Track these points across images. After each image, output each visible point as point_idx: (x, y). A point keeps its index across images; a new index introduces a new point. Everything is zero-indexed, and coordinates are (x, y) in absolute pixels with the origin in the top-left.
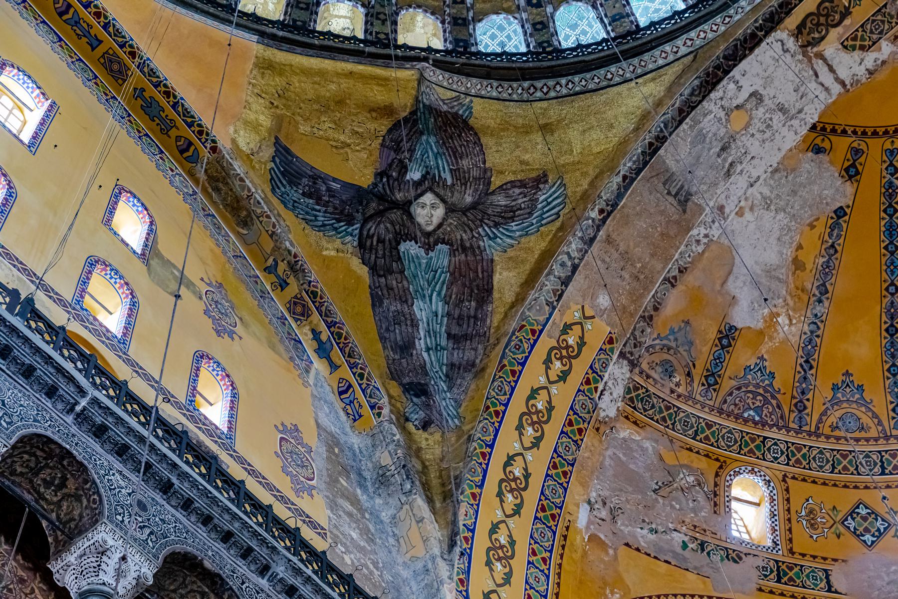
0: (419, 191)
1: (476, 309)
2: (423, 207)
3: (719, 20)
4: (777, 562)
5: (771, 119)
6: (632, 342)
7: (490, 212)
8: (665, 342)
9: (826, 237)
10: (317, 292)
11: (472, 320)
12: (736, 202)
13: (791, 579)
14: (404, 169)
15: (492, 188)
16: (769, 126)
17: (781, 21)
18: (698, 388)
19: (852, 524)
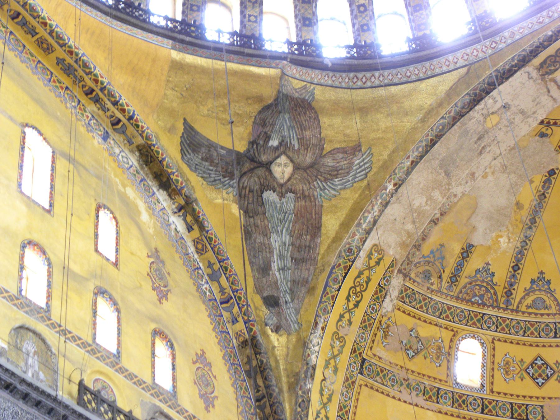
0: (277, 154)
1: (310, 241)
2: (279, 166)
3: (488, 43)
4: (482, 399)
5: (514, 119)
6: (406, 262)
7: (322, 170)
8: (427, 259)
9: (540, 188)
10: (212, 238)
11: (307, 249)
12: (483, 169)
13: (490, 411)
14: (268, 138)
15: (324, 153)
16: (512, 123)
17: (530, 61)
18: (445, 284)
19: (531, 371)
